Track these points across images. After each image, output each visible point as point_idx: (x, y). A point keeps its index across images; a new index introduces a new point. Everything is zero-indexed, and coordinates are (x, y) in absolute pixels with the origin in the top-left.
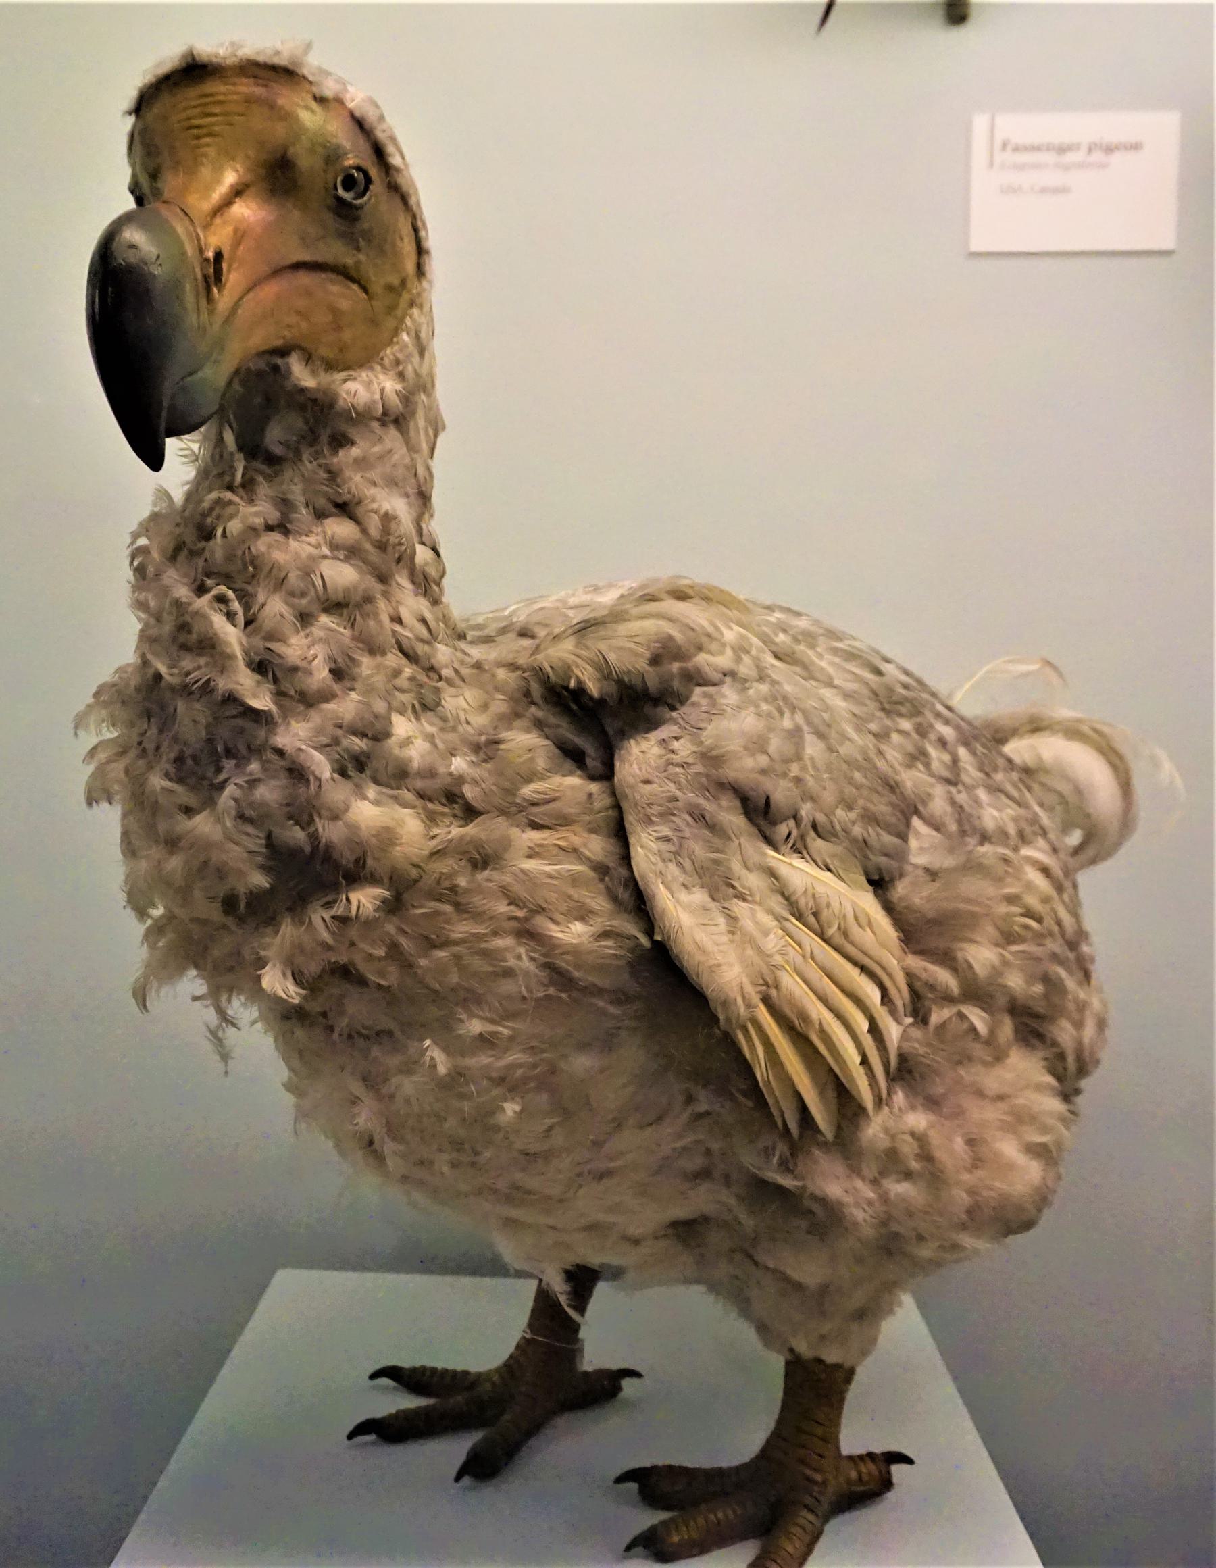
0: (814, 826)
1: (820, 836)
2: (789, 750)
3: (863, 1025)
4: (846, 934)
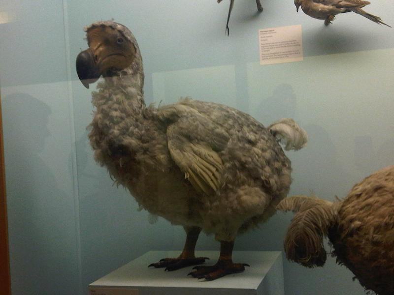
3: (211, 174)
4: (206, 158)
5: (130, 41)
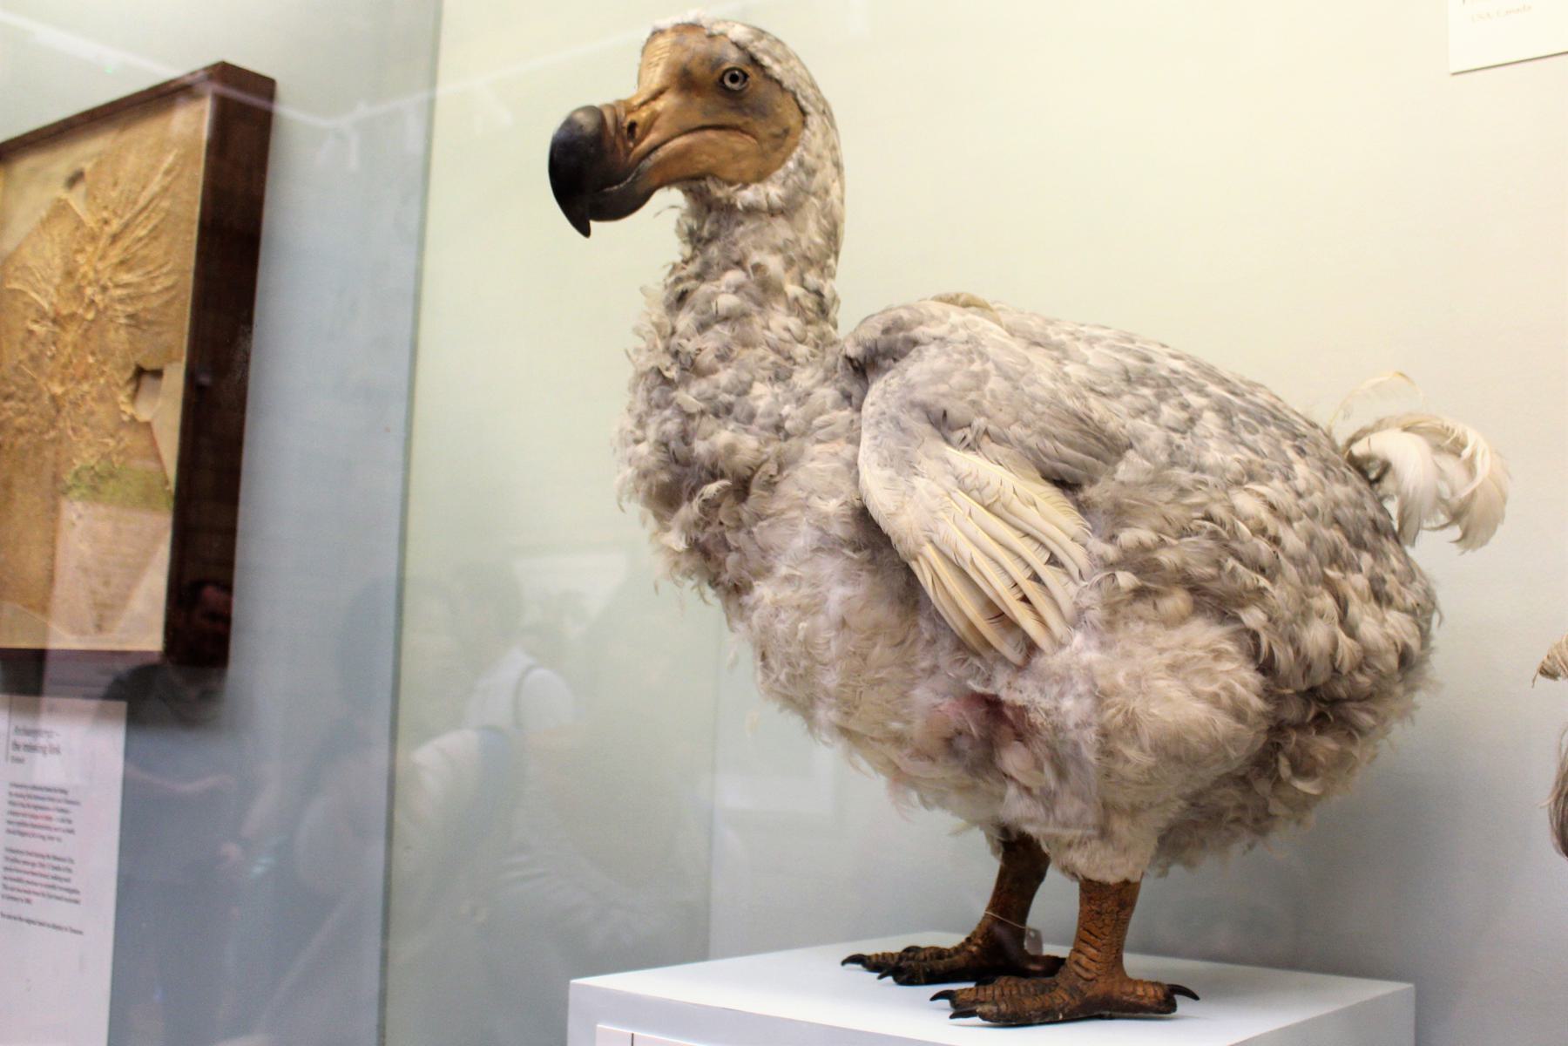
0: (986, 432)
1: (993, 441)
2: (969, 382)
3: (1021, 576)
5: (779, 83)
